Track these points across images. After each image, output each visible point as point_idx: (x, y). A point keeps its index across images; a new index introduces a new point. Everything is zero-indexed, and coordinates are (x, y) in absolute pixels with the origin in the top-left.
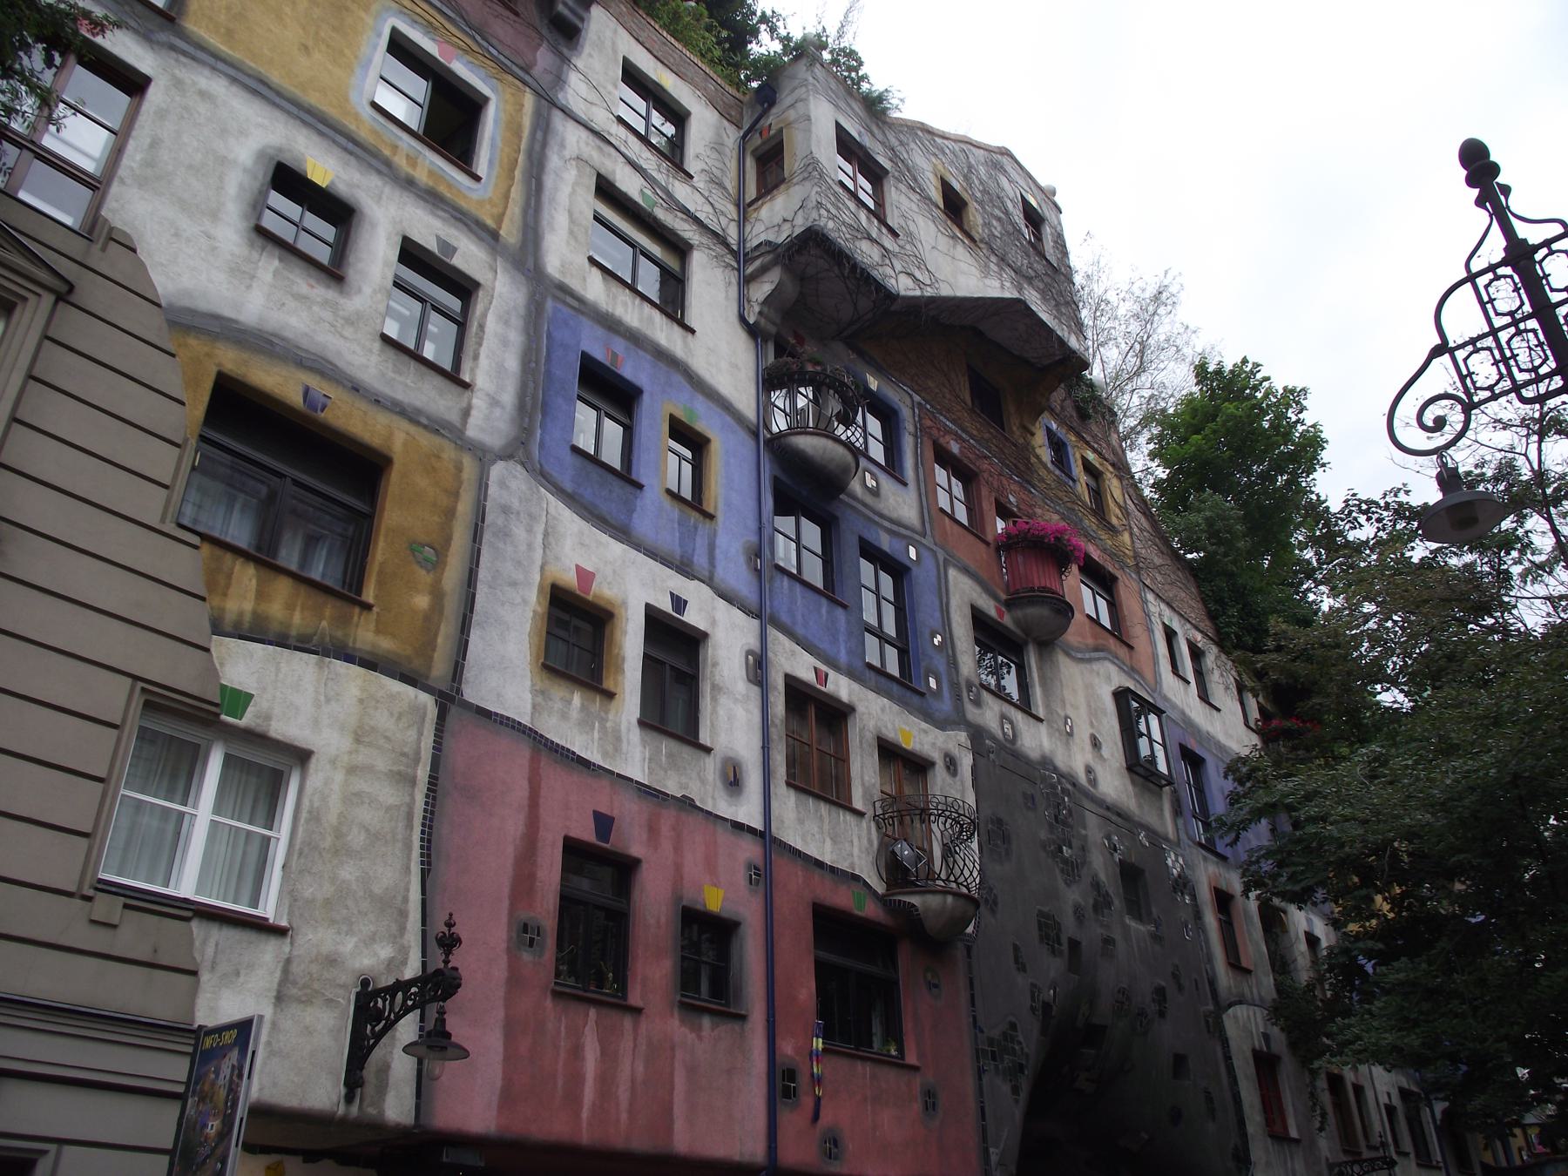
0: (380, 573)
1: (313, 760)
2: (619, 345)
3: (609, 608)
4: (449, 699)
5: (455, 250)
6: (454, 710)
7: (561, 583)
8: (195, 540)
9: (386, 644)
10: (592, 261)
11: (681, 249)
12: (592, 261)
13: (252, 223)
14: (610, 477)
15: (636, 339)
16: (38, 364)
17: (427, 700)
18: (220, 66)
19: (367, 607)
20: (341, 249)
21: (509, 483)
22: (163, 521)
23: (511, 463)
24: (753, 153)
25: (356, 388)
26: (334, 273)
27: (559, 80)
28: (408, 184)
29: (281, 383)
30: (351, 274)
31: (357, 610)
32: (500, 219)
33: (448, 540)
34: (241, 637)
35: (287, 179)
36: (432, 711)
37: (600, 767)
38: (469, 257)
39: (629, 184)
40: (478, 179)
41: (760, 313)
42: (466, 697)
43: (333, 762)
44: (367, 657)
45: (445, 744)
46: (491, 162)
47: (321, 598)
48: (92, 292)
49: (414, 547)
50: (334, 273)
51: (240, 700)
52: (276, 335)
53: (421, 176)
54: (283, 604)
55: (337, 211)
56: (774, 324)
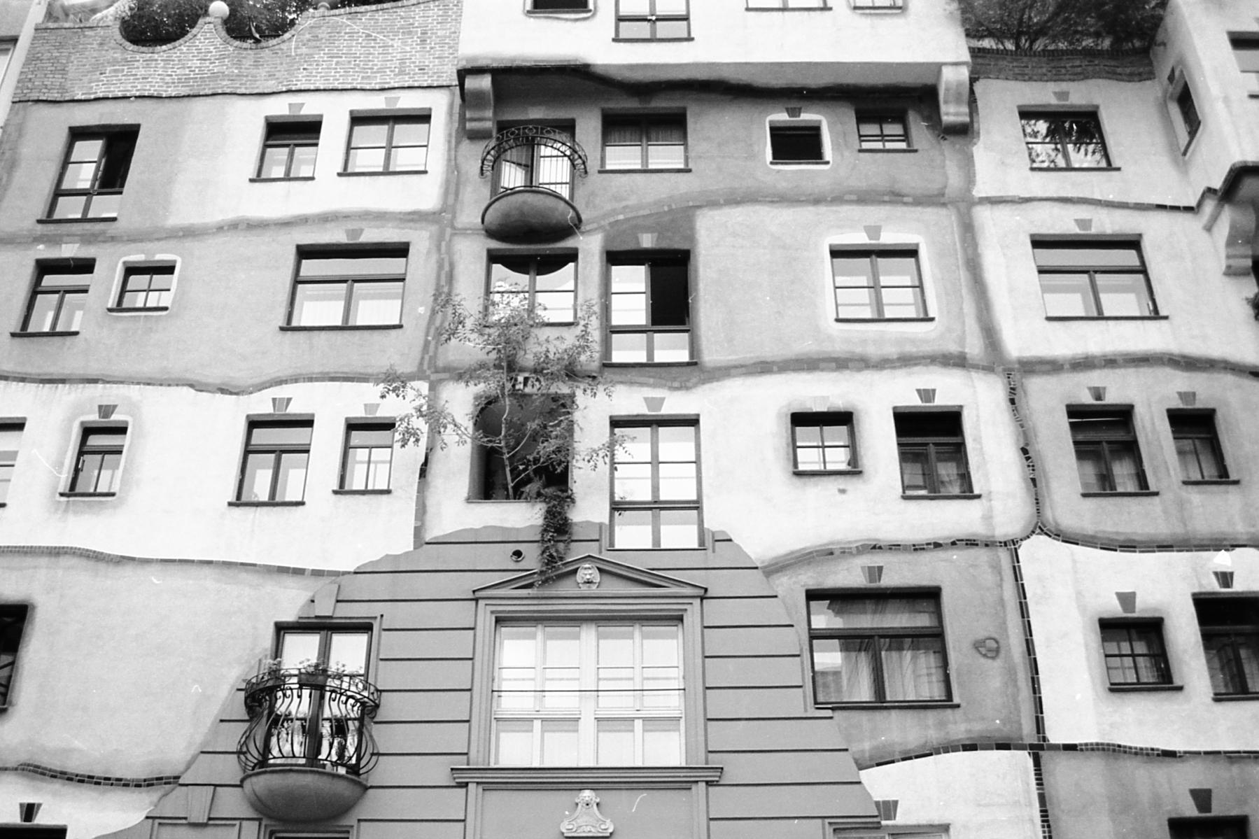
0: (959, 675)
1: (952, 830)
2: (1096, 378)
3: (1157, 615)
4: (1039, 749)
5: (934, 391)
6: (1045, 755)
7: (1106, 616)
8: (829, 713)
9: (977, 728)
10: (1049, 319)
11: (1133, 243)
12: (1049, 319)
13: (791, 469)
14: (1126, 500)
15: (1110, 362)
16: (706, 648)
17: (1024, 759)
18: (733, 371)
19: (958, 706)
20: (853, 446)
21: (1039, 555)
22: (806, 710)
23: (1034, 537)
24: (1171, 98)
25: (895, 547)
26: (854, 470)
27: (970, 179)
28: (883, 364)
29: (850, 576)
30: (866, 462)
31: (949, 711)
32: (962, 340)
33: (1003, 626)
34: (879, 765)
35: (801, 419)
36: (1030, 762)
37: (1186, 752)
38: (948, 389)
39: (1063, 222)
40: (932, 319)
41: (1228, 257)
42: (1052, 741)
43: (965, 827)
44: (968, 742)
45: (1045, 782)
46: (938, 296)
47: (922, 713)
48: (717, 583)
49: (978, 645)
50: (854, 470)
51: (889, 808)
52: (832, 543)
53: (892, 351)
54: (898, 729)
55: (843, 418)
56: (1246, 257)
